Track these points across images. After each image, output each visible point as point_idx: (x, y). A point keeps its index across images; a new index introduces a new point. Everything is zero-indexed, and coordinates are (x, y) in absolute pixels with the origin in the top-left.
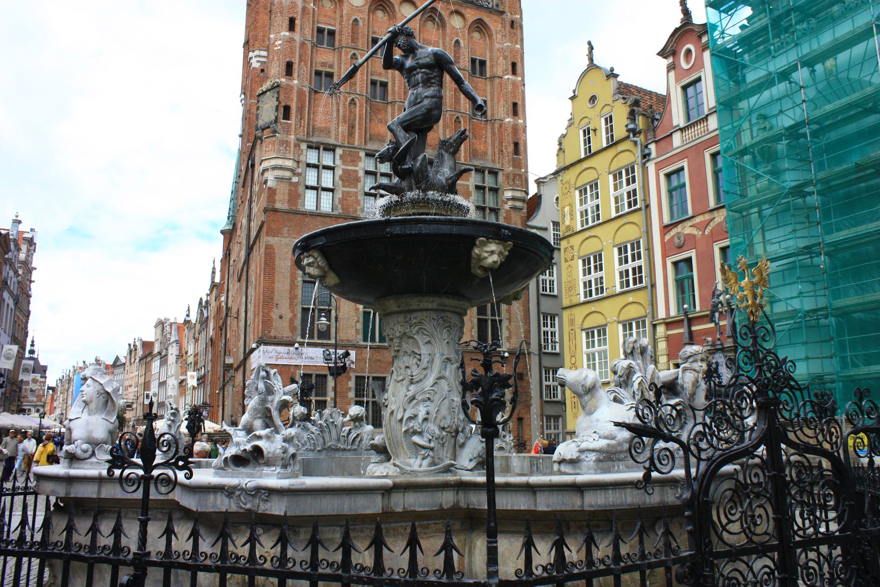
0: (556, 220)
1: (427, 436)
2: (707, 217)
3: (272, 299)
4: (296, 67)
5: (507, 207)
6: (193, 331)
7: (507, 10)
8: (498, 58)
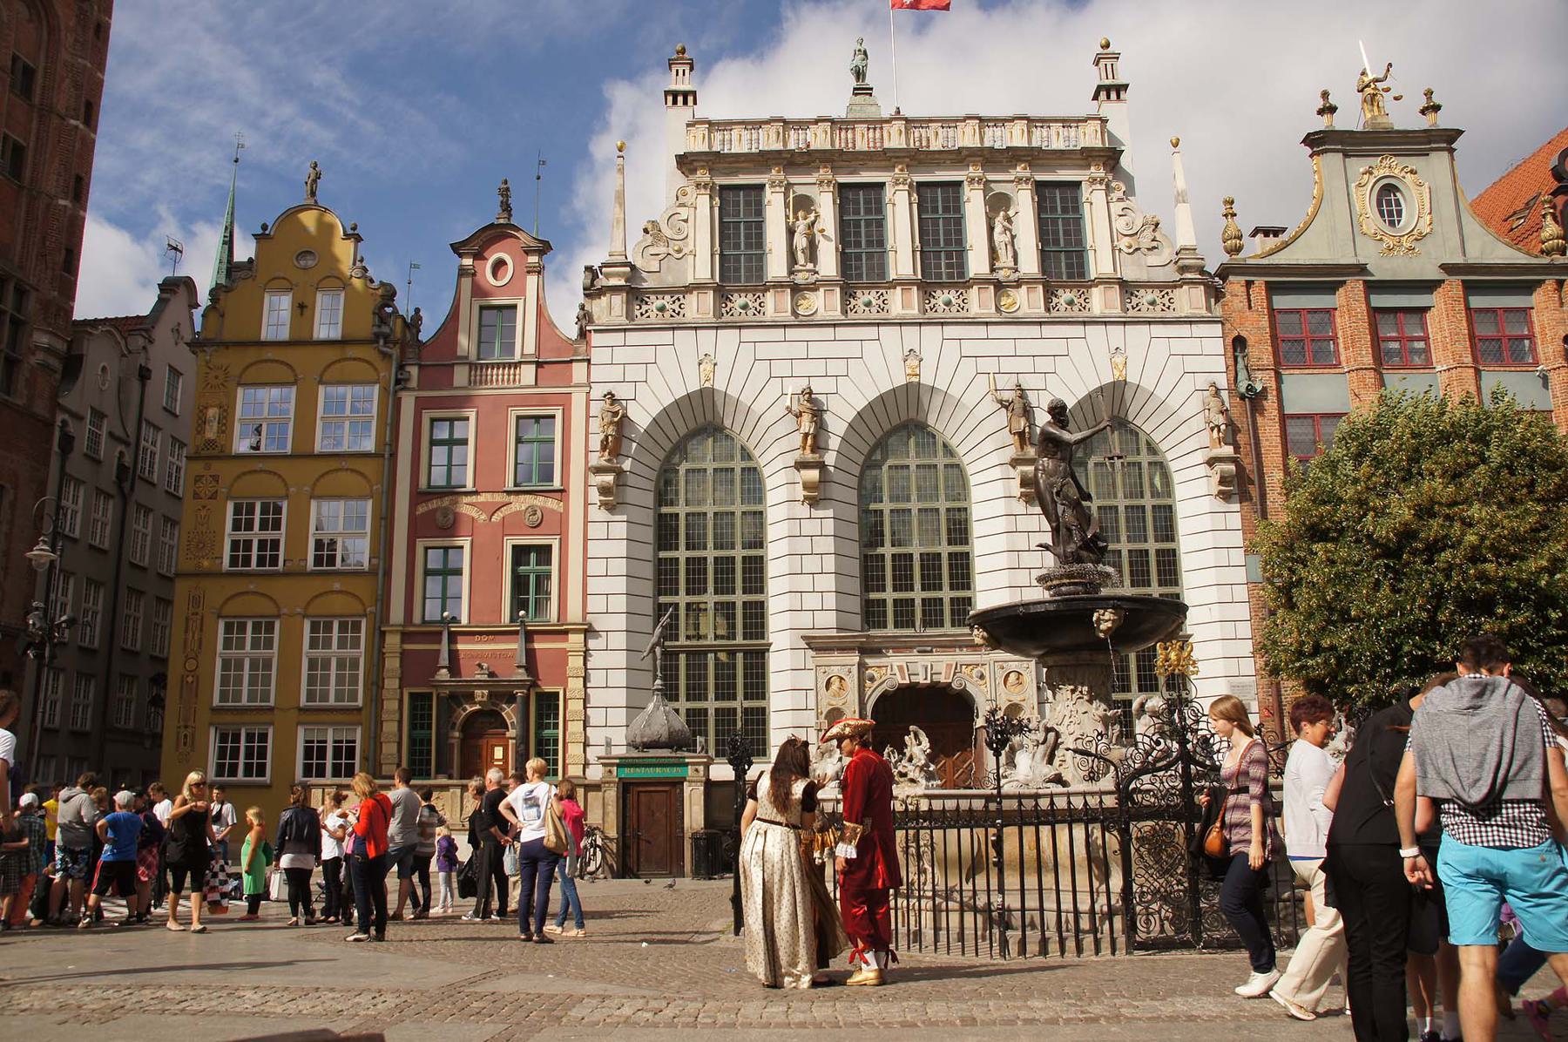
2: (499, 498)
5: (33, 360)
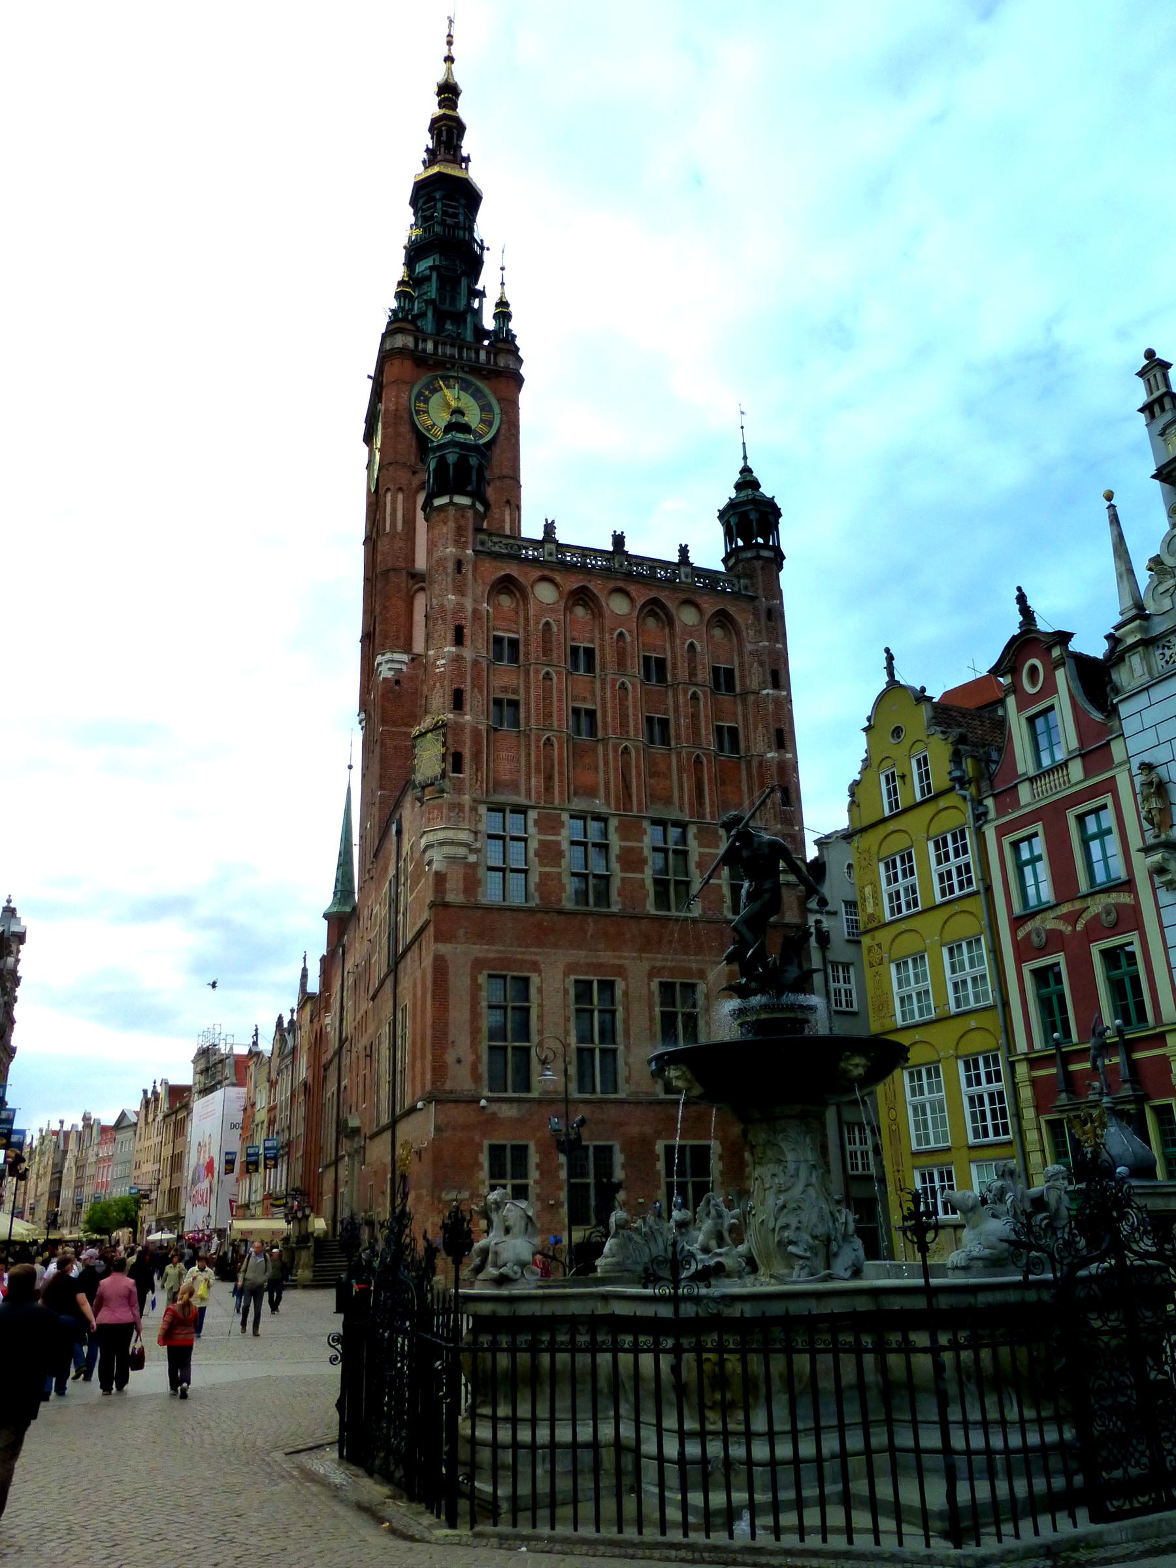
0: (849, 899)
1: (803, 1246)
2: (1078, 905)
3: (446, 1034)
4: (467, 696)
6: (265, 1070)
7: (760, 592)
8: (751, 665)
